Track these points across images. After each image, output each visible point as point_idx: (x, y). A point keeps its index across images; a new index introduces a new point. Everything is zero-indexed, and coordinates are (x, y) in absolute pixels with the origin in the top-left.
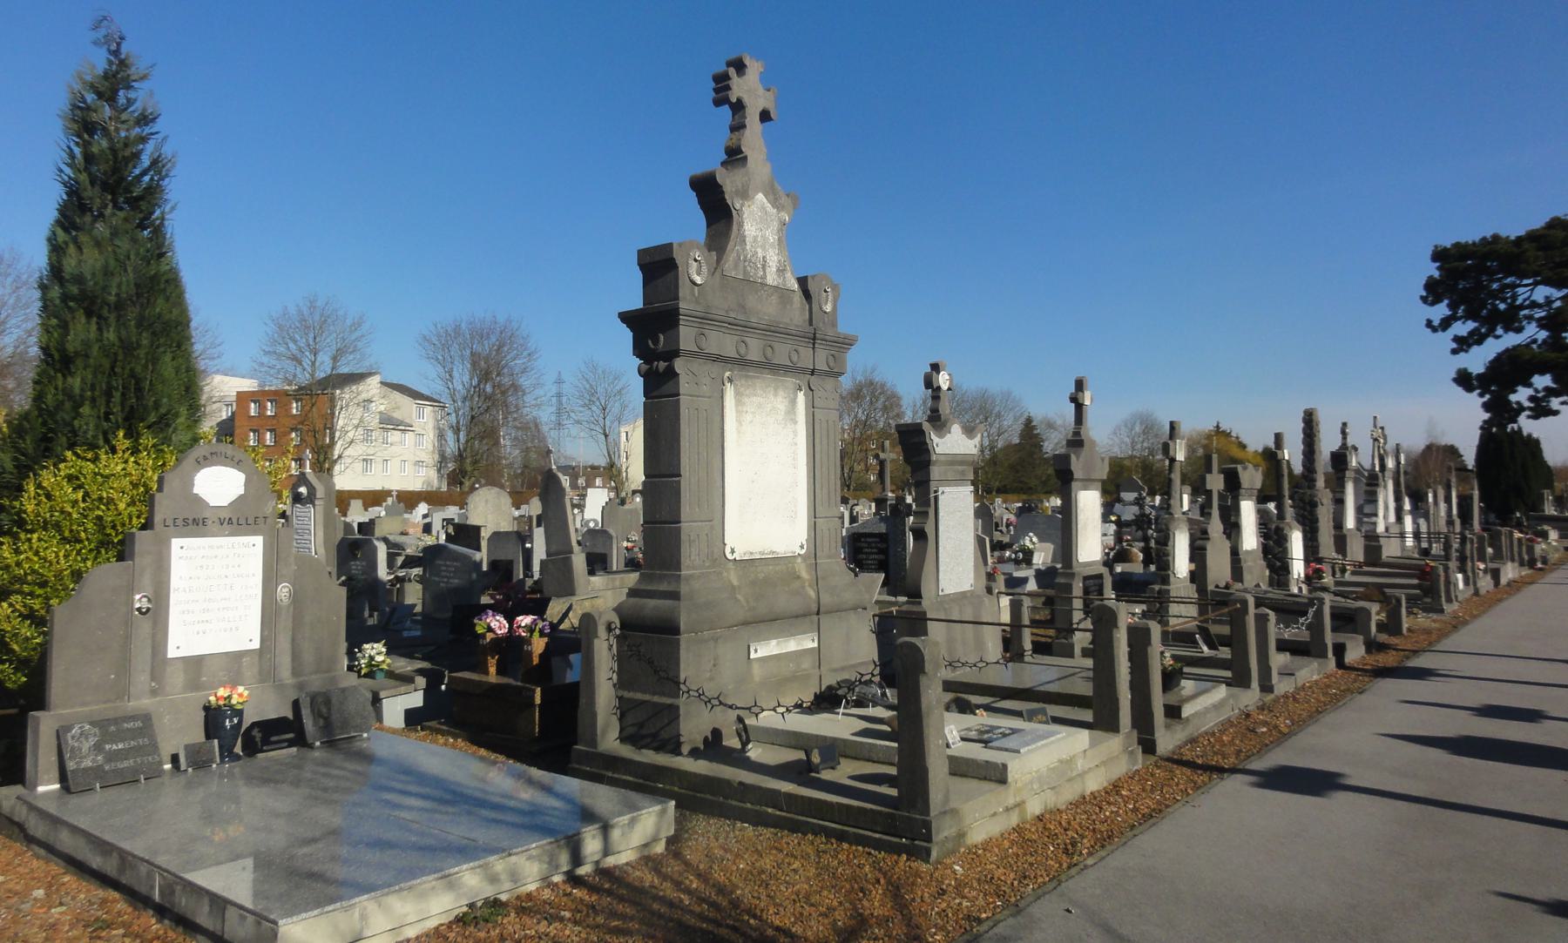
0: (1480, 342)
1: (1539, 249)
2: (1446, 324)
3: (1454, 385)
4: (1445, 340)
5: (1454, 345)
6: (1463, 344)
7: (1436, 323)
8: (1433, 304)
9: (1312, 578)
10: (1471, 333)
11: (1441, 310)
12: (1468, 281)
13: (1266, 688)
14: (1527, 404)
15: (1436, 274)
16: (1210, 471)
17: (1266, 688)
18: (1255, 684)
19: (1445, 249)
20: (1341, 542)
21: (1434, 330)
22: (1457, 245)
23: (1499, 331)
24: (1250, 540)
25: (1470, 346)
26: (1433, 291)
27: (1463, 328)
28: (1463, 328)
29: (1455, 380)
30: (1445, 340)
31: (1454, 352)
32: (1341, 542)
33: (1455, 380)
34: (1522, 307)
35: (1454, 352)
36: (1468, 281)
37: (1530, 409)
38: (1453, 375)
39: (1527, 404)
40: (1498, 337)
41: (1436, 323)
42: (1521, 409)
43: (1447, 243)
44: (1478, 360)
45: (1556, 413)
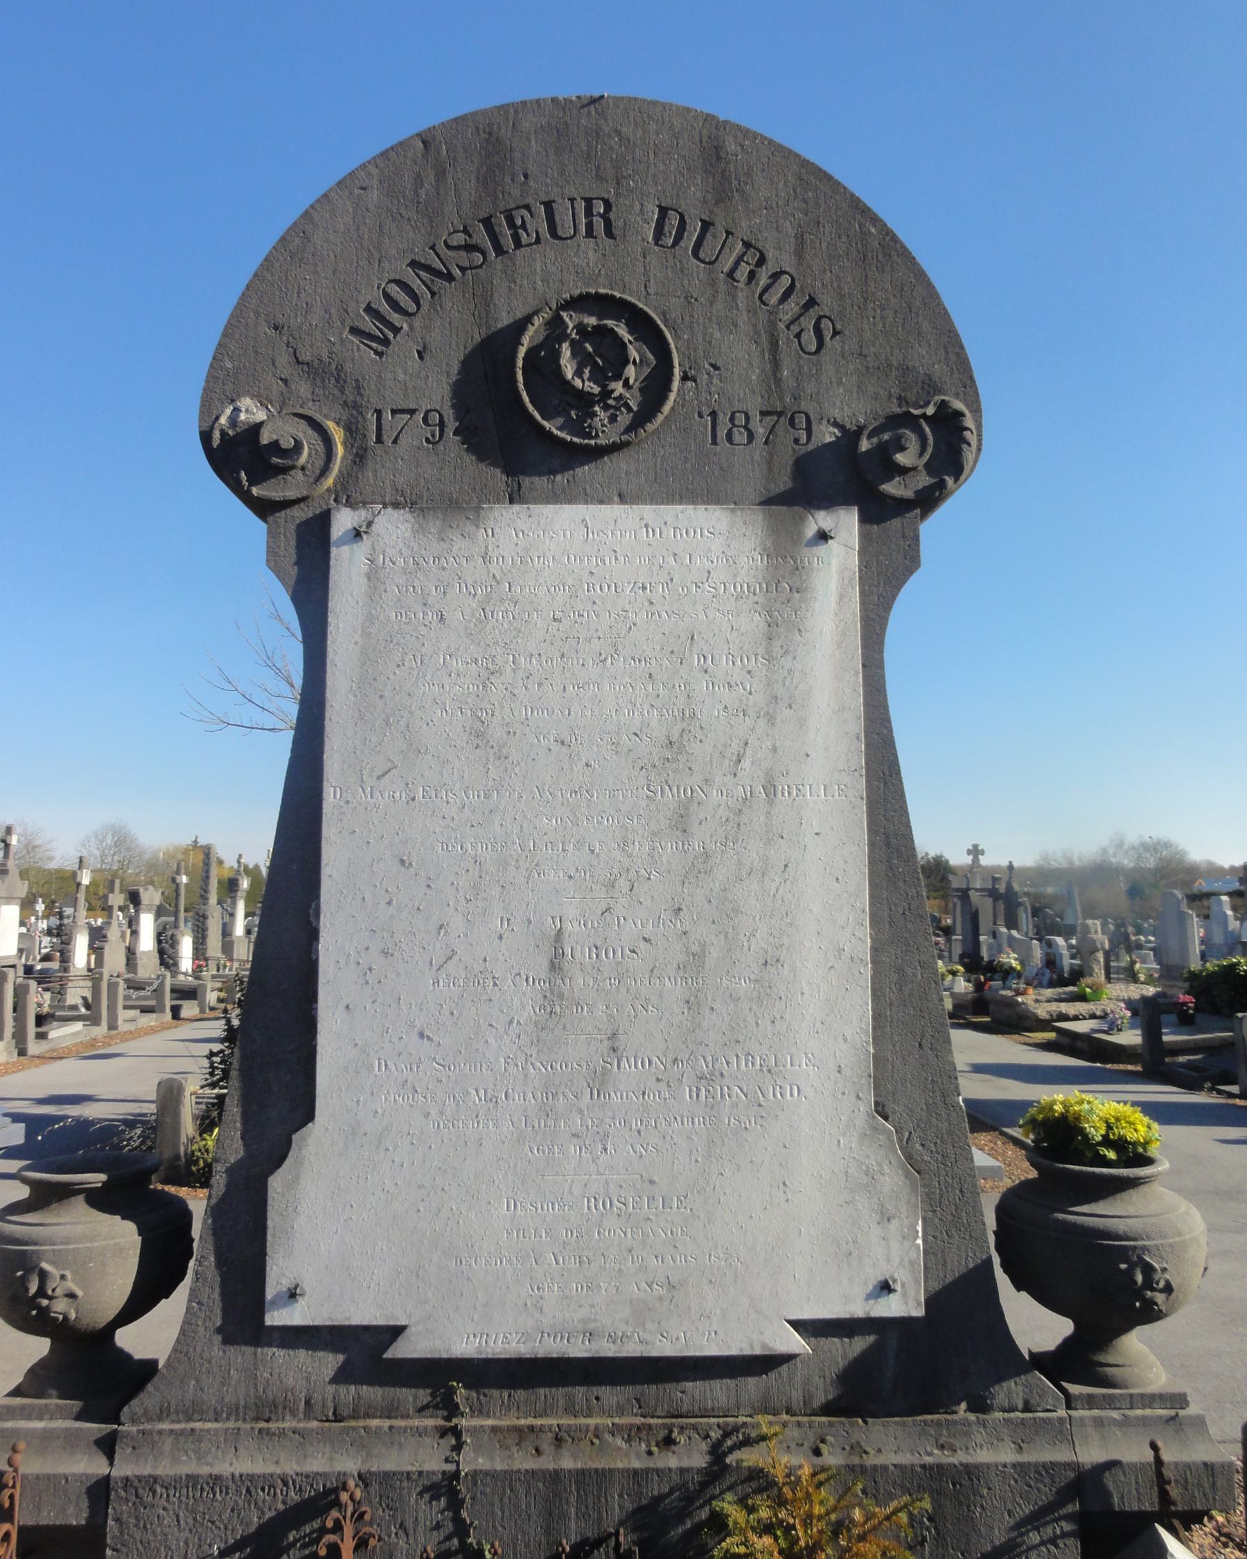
9: (197, 972)
13: (112, 1026)
16: (112, 891)
17: (112, 1026)
18: (104, 1023)
20: (227, 947)
24: (147, 942)
32: (227, 947)
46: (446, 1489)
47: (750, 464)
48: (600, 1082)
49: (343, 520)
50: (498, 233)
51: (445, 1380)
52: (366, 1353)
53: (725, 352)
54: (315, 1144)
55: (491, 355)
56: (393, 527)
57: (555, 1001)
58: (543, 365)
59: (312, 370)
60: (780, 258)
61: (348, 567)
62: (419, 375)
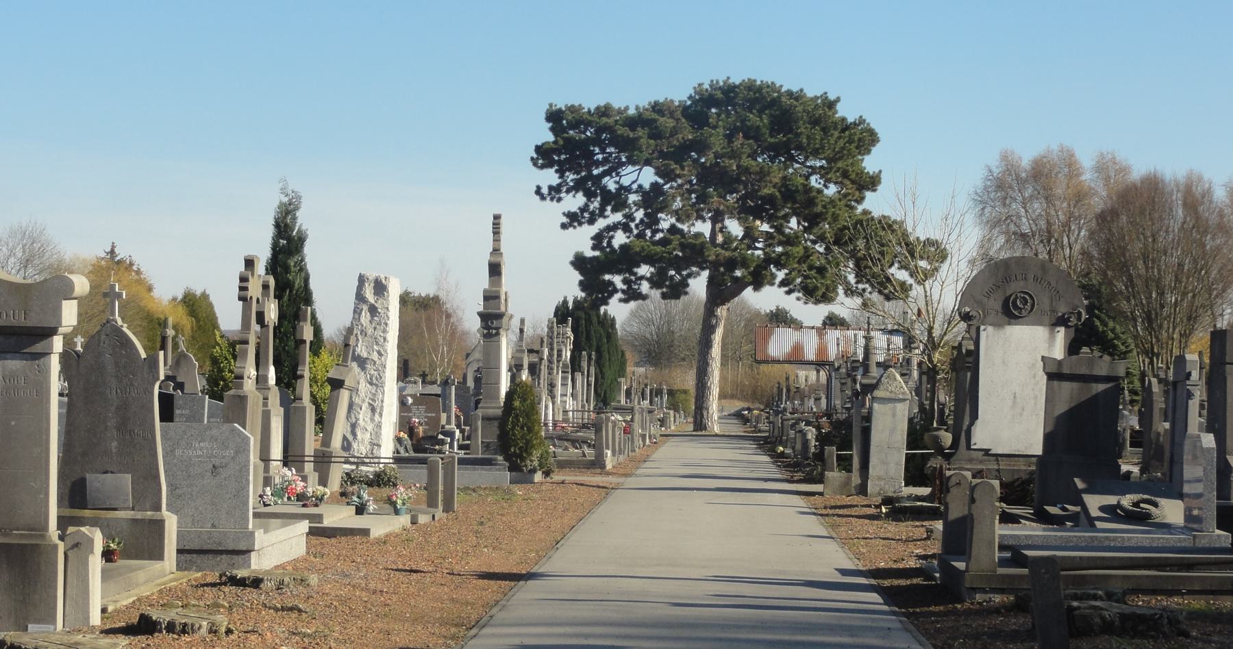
0: (591, 221)
1: (650, 137)
2: (555, 192)
3: (572, 268)
4: (556, 211)
5: (565, 220)
6: (573, 219)
7: (545, 191)
8: (542, 167)
10: (584, 209)
11: (550, 177)
12: (578, 147)
14: (620, 285)
15: (551, 138)
19: (560, 111)
21: (543, 198)
22: (572, 109)
23: (608, 212)
25: (580, 224)
26: (544, 156)
27: (574, 202)
28: (574, 202)
29: (572, 263)
30: (556, 211)
31: (564, 226)
33: (572, 263)
34: (628, 190)
35: (564, 226)
36: (578, 147)
37: (623, 291)
38: (571, 258)
39: (620, 285)
40: (605, 217)
41: (545, 191)
42: (616, 291)
43: (561, 104)
44: (582, 240)
45: (644, 297)
46: (998, 470)
47: (1046, 319)
48: (1021, 415)
49: (982, 328)
50: (1007, 280)
51: (997, 456)
52: (986, 452)
53: (1043, 301)
54: (978, 423)
55: (1006, 301)
56: (990, 329)
57: (1014, 402)
58: (1014, 303)
59: (977, 302)
60: (1053, 284)
61: (983, 335)
62: (995, 304)
